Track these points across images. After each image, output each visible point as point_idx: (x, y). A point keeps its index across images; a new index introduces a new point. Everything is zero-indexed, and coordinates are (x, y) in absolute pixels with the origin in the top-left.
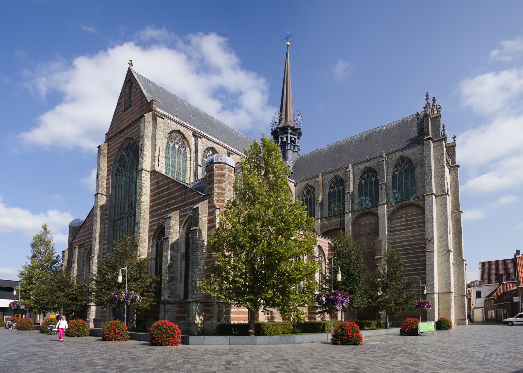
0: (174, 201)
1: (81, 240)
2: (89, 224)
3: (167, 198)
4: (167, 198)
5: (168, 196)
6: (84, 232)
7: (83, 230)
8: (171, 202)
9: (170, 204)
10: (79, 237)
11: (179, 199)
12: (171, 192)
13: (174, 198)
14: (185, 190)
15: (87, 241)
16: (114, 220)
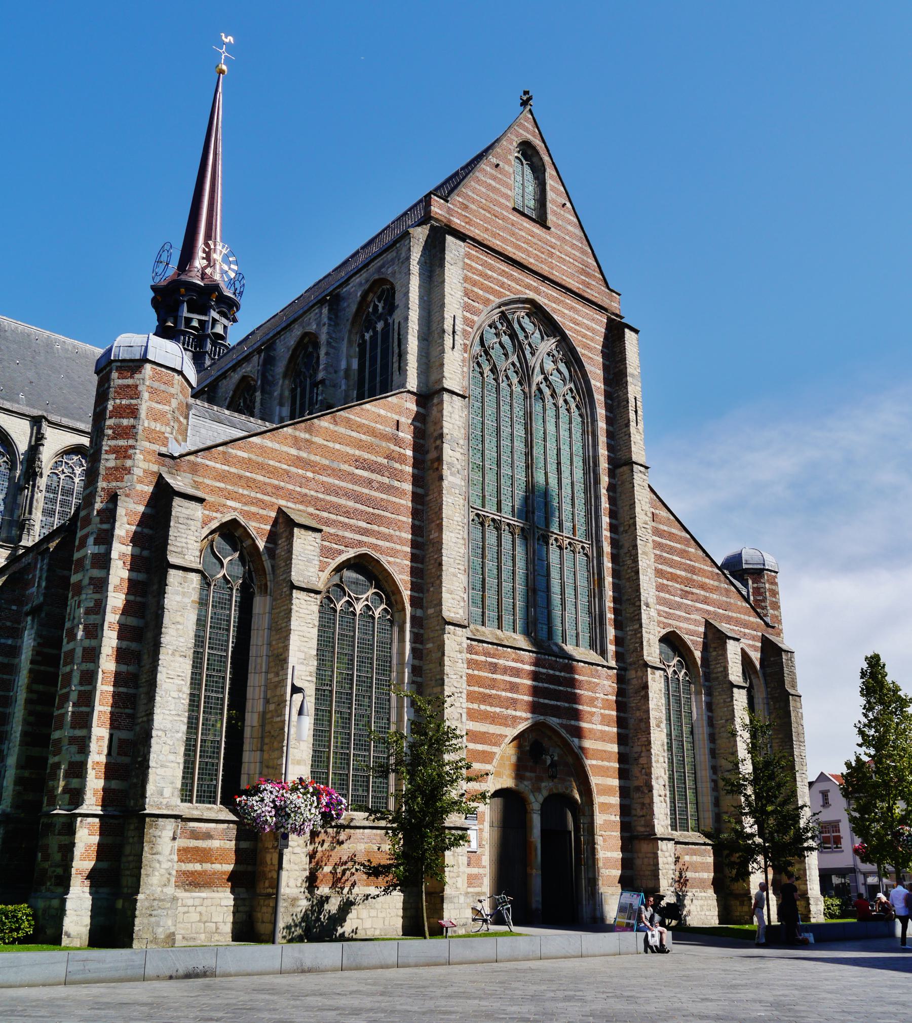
0: (702, 593)
1: (277, 488)
2: (338, 446)
3: (683, 573)
4: (683, 573)
5: (685, 570)
6: (299, 462)
7: (294, 451)
8: (695, 590)
9: (692, 593)
10: (248, 464)
11: (715, 596)
12: (694, 567)
13: (702, 587)
14: (726, 586)
15: (325, 514)
16: (478, 515)
